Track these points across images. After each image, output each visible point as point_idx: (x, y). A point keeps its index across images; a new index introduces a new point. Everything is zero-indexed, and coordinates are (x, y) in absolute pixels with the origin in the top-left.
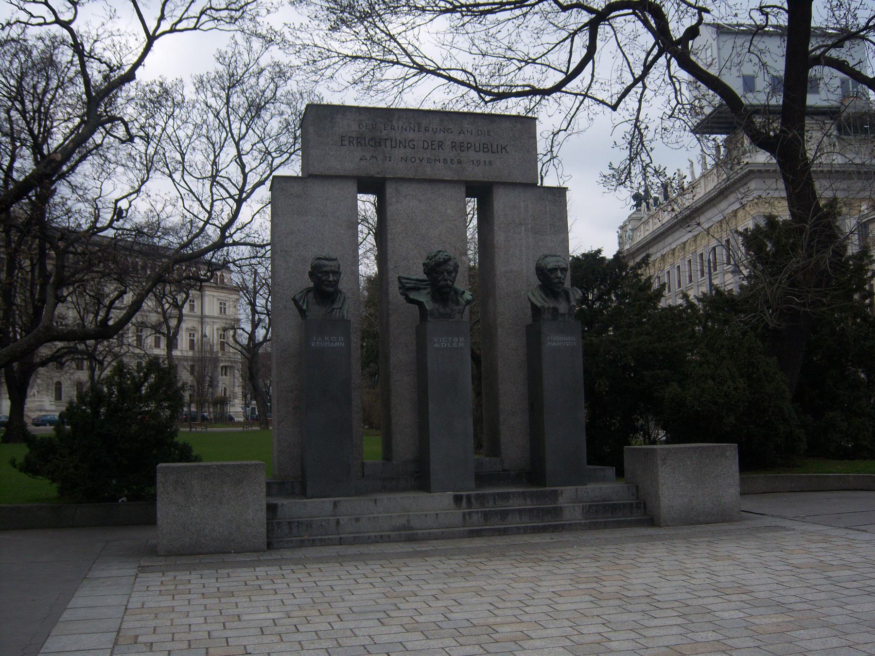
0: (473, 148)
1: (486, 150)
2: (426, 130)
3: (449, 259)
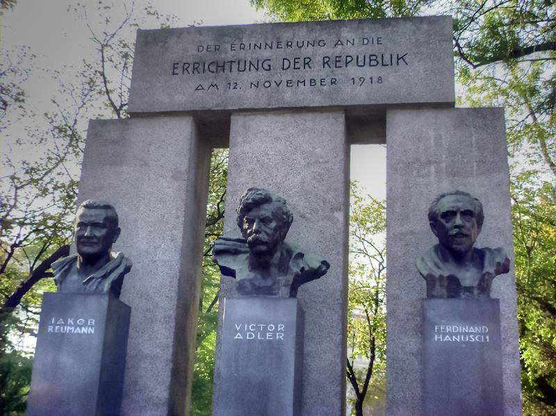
0: (355, 61)
1: (373, 63)
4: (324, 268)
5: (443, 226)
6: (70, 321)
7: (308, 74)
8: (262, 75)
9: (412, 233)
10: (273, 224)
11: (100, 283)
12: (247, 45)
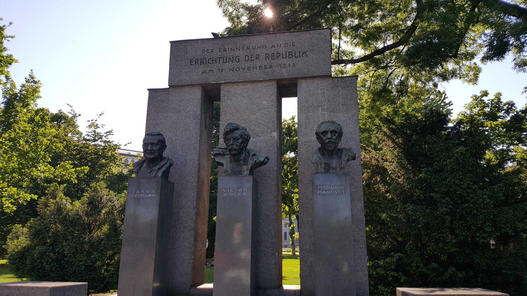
2: (248, 48)
3: (237, 129)
4: (267, 160)
5: (322, 138)
6: (143, 191)
7: (258, 63)
8: (236, 65)
9: (310, 142)
10: (240, 141)
11: (157, 172)
12: (227, 49)
